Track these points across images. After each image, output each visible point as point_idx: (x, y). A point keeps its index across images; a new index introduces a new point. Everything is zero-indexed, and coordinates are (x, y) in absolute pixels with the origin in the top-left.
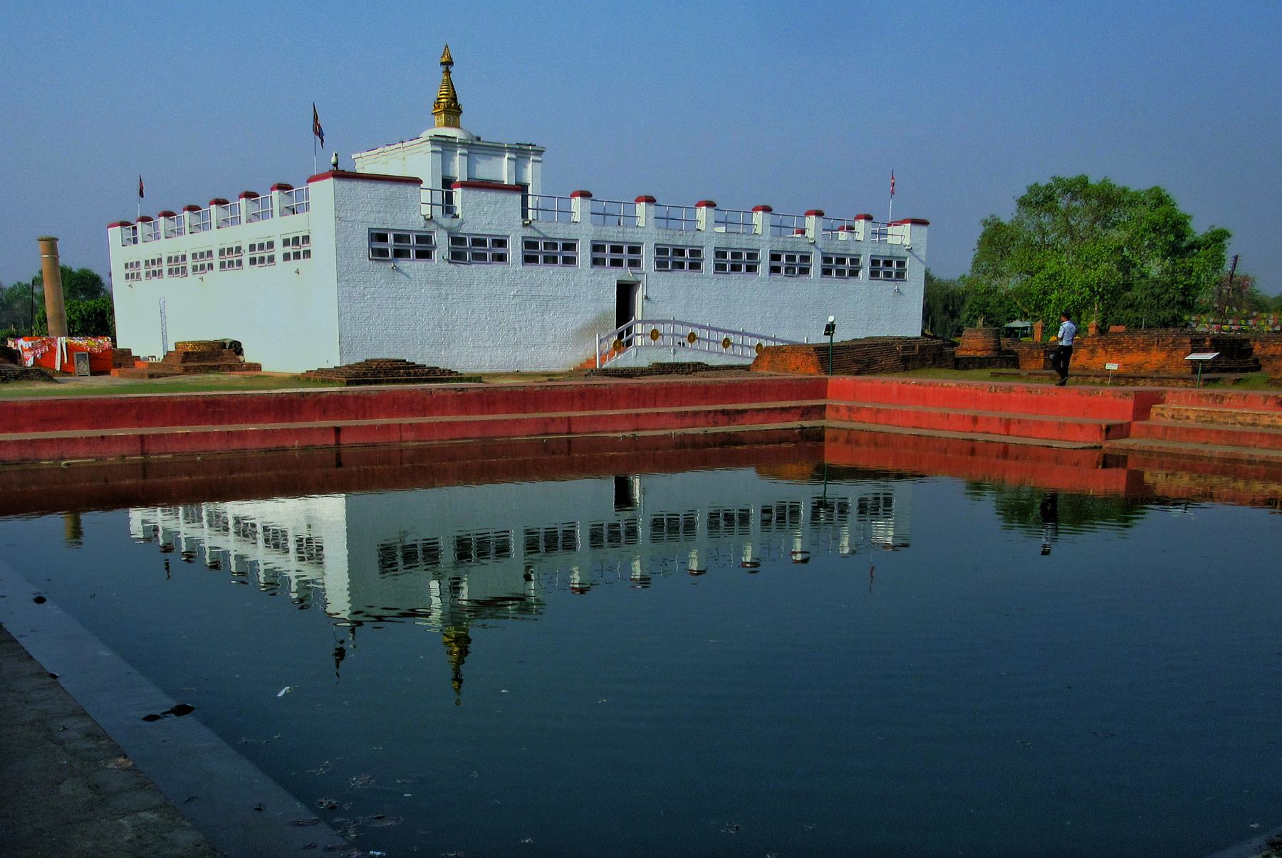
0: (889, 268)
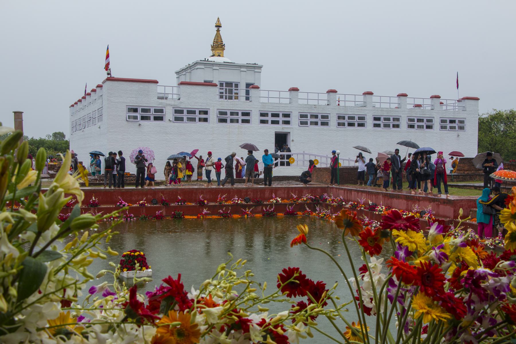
0: (453, 124)
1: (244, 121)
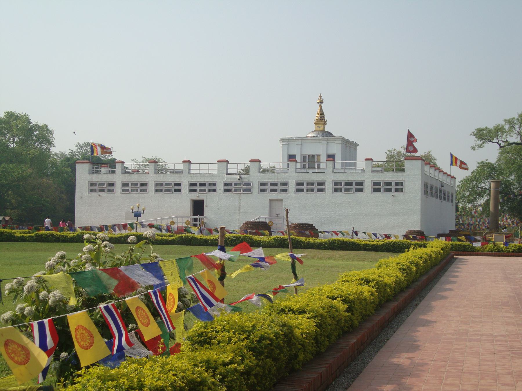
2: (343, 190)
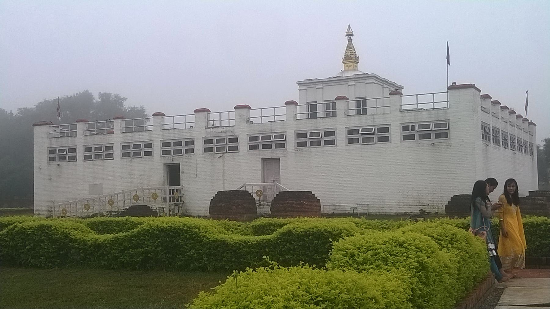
1: (328, 143)
2: (361, 140)
